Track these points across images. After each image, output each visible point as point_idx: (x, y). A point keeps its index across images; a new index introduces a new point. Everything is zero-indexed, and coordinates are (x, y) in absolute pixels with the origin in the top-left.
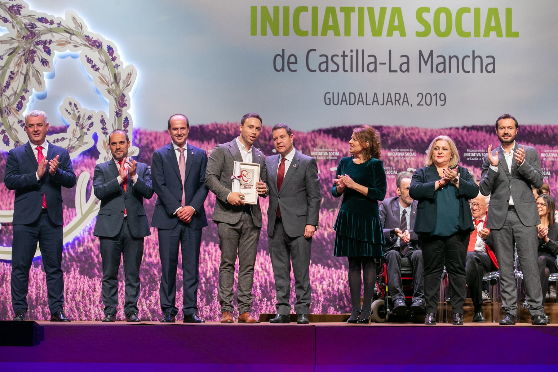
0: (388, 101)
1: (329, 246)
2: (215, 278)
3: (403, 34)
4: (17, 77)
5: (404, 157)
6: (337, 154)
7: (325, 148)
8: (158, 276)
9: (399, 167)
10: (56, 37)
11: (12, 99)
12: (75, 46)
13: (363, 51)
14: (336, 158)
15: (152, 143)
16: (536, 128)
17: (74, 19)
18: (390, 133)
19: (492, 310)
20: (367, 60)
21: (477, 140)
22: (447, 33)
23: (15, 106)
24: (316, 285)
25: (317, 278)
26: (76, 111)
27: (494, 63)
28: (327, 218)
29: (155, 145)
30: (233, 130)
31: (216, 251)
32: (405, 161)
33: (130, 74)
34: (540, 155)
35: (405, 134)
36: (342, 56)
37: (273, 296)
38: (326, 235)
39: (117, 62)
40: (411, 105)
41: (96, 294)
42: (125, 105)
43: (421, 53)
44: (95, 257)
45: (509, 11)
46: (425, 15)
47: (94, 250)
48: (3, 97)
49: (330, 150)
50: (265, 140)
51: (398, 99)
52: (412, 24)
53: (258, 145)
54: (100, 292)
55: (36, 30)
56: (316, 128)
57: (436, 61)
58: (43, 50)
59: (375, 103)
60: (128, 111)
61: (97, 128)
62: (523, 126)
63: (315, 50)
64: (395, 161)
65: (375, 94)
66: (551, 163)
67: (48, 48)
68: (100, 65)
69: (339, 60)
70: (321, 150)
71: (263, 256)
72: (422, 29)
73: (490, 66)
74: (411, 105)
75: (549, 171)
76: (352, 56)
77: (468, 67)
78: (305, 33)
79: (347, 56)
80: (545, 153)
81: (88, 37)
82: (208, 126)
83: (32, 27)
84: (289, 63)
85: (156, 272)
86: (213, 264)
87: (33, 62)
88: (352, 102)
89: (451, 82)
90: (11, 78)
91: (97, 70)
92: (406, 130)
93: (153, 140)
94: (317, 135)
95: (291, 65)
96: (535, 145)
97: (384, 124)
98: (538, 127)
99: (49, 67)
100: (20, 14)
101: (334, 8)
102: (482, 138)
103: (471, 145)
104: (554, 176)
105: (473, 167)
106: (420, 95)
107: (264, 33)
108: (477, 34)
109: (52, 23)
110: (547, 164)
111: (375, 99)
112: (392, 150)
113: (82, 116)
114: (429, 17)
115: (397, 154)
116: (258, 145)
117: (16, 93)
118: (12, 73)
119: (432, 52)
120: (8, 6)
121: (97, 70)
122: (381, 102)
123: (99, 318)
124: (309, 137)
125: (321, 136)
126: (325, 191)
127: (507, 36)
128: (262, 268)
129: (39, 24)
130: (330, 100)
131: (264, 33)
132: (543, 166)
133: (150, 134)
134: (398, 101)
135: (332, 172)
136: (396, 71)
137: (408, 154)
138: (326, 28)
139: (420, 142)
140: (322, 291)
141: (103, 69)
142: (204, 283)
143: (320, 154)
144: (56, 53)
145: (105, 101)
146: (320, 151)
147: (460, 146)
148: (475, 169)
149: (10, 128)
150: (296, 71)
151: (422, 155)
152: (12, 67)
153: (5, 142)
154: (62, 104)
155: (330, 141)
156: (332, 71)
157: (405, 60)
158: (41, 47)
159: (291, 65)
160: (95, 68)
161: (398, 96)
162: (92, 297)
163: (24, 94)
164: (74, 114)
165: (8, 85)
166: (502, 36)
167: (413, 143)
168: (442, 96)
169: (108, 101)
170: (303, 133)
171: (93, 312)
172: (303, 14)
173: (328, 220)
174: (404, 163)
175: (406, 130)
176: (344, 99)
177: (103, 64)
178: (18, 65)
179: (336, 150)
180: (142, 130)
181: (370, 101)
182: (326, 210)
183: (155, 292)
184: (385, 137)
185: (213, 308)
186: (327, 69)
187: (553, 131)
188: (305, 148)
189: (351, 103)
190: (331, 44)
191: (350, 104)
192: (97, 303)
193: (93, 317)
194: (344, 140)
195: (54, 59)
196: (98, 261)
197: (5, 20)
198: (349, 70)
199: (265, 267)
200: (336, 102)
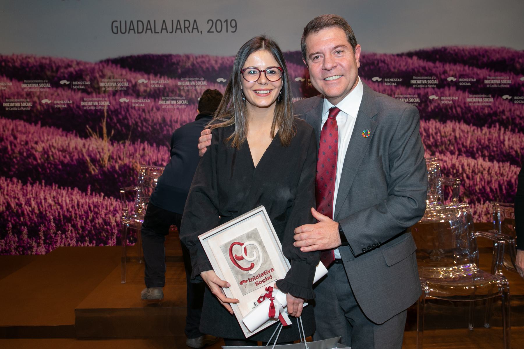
1: (121, 178)
2: (8, 213)
5: (195, 86)
6: (126, 84)
7: (113, 78)
9: (190, 96)
14: (126, 89)
18: (180, 61)
24: (109, 217)
25: (110, 211)
28: (118, 150)
30: (19, 62)
31: (8, 185)
32: (196, 90)
35: (195, 62)
37: (67, 229)
38: (117, 168)
40: (201, 32)
49: (120, 80)
50: (52, 71)
56: (104, 57)
64: (186, 91)
65: (164, 21)
70: (109, 80)
71: (55, 189)
74: (201, 32)
86: (5, 199)
88: (140, 31)
92: (197, 58)
94: (105, 66)
97: (174, 52)
106: (210, 22)
111: (164, 27)
112: (182, 79)
115: (187, 83)
122: (170, 30)
124: (97, 67)
125: (109, 67)
126: (114, 123)
128: (54, 201)
134: (187, 28)
135: (122, 103)
137: (198, 83)
139: (211, 70)
140: (115, 224)
143: (109, 84)
146: (108, 82)
151: (213, 84)
155: (118, 71)
161: (187, 23)
173: (119, 152)
174: (195, 92)
175: (197, 58)
176: (132, 28)
179: (125, 80)
181: (158, 29)
182: (116, 142)
184: (174, 66)
185: (8, 241)
189: (140, 31)
191: (138, 33)
199: (58, 200)
200: (123, 31)
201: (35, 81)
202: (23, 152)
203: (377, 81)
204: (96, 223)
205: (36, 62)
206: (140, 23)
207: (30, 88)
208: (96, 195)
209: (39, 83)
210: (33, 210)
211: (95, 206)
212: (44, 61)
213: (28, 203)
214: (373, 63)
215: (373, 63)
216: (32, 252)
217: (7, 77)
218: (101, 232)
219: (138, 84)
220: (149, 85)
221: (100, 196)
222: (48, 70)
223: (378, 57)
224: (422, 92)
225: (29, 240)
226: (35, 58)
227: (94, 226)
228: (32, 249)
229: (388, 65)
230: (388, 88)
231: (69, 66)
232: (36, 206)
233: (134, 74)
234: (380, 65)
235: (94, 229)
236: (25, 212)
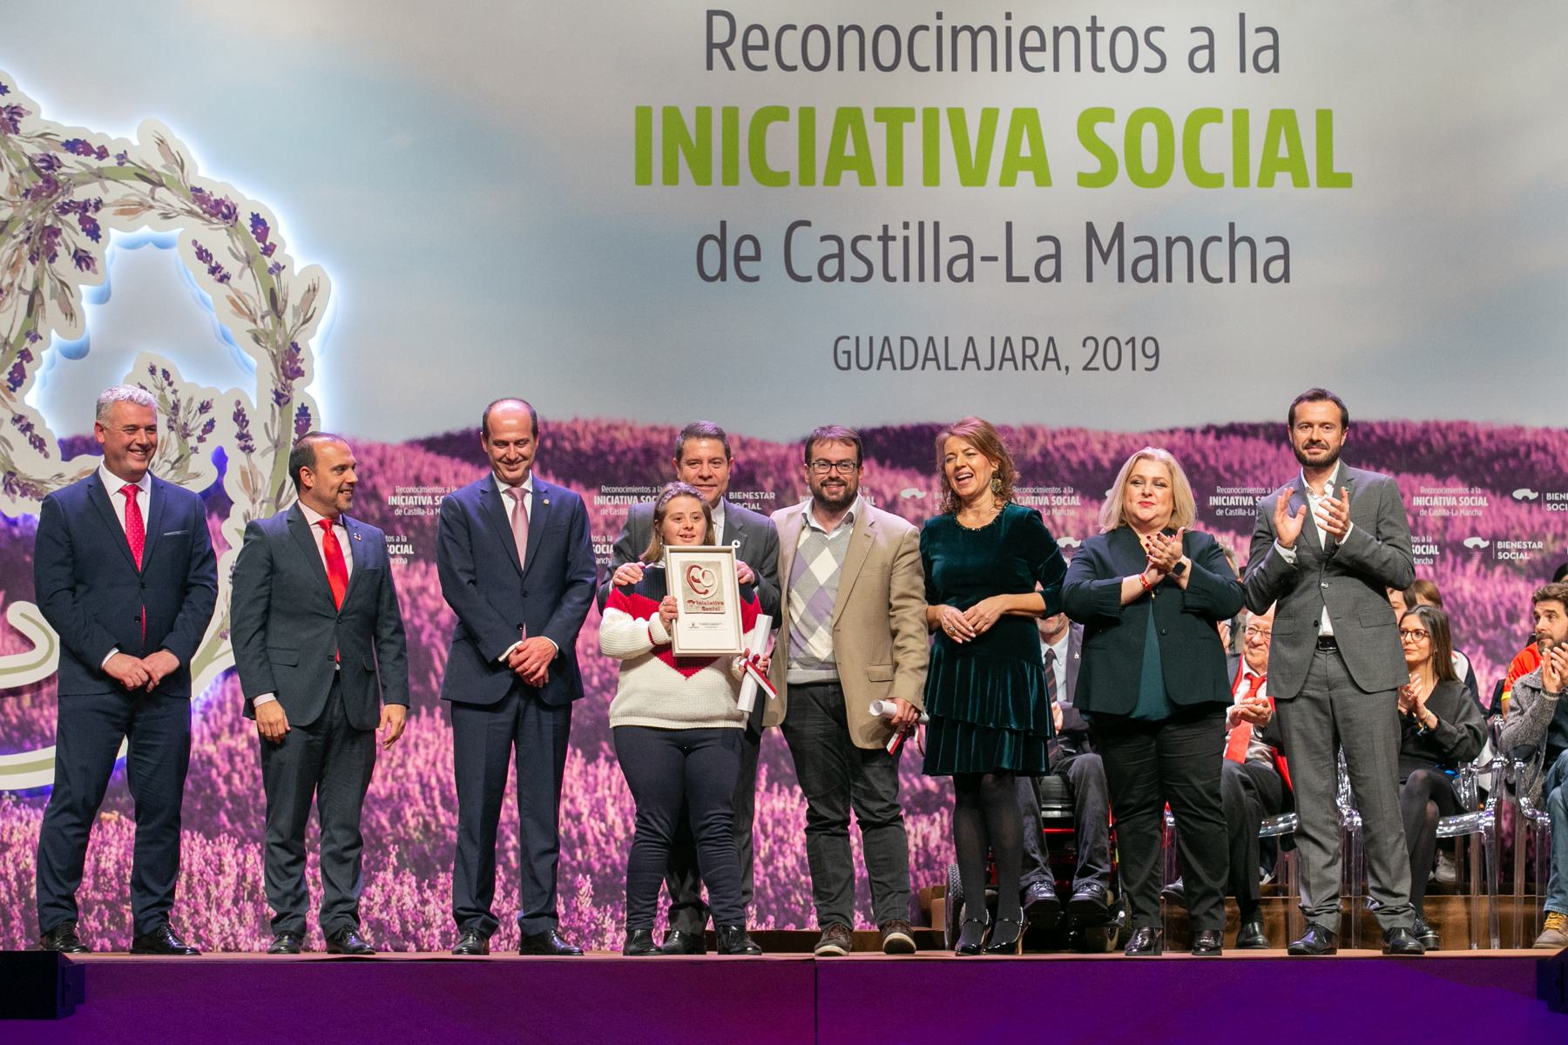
0: (1003, 359)
3: (1043, 179)
5: (1049, 507)
8: (389, 830)
10: (114, 192)
12: (166, 216)
13: (936, 225)
15: (371, 473)
16: (1400, 430)
19: (1286, 915)
20: (949, 250)
21: (1242, 463)
22: (1161, 177)
26: (168, 390)
27: (1286, 257)
29: (380, 480)
30: (589, 438)
33: (313, 290)
34: (1411, 501)
35: (1050, 447)
36: (880, 238)
41: (224, 881)
42: (299, 373)
43: (1091, 230)
44: (220, 781)
45: (1324, 119)
46: (1101, 130)
47: (219, 762)
51: (1033, 354)
52: (1066, 154)
53: (658, 480)
54: (234, 875)
55: (60, 175)
57: (1133, 250)
58: (79, 228)
59: (971, 365)
60: (307, 390)
61: (224, 433)
62: (1365, 424)
63: (808, 224)
65: (971, 339)
66: (1440, 524)
67: (93, 221)
68: (231, 266)
69: (872, 250)
72: (1093, 165)
75: (1434, 543)
76: (906, 239)
77: (1218, 266)
78: (782, 179)
79: (894, 239)
80: (1425, 495)
81: (200, 190)
83: (50, 167)
84: (738, 259)
85: (385, 822)
87: (52, 260)
88: (908, 362)
91: (224, 278)
92: (1054, 436)
93: (376, 466)
95: (744, 265)
96: (1397, 473)
98: (1404, 427)
99: (95, 272)
100: (17, 131)
101: (858, 111)
102: (1258, 457)
103: (1228, 476)
104: (1449, 556)
105: (1232, 533)
106: (1091, 343)
107: (671, 178)
108: (1241, 179)
109: (102, 154)
110: (1430, 526)
111: (971, 355)
113: (183, 404)
114: (1112, 134)
116: (658, 480)
119: (1120, 226)
121: (224, 278)
122: (985, 361)
123: (232, 946)
127: (1321, 184)
129: (67, 158)
130: (849, 357)
131: (671, 178)
132: (1420, 531)
133: (368, 451)
134: (1031, 357)
136: (1026, 279)
137: (1059, 501)
138: (838, 163)
139: (1090, 466)
141: (240, 277)
142: (514, 848)
144: (115, 235)
147: (1196, 477)
148: (1239, 540)
150: (756, 279)
151: (1095, 502)
156: (854, 279)
157: (1049, 248)
158: (73, 218)
159: (744, 265)
160: (218, 276)
161: (1030, 346)
162: (212, 888)
163: (27, 344)
166: (1307, 185)
167: (1072, 471)
168: (1150, 344)
169: (253, 361)
170: (778, 446)
171: (216, 928)
172: (774, 128)
175: (1054, 436)
176: (887, 355)
177: (241, 265)
181: (956, 360)
183: (381, 874)
186: (840, 275)
187: (1445, 437)
188: (782, 485)
190: (853, 208)
191: (903, 368)
192: (228, 904)
193: (216, 941)
194: (888, 463)
195: (108, 252)
196: (230, 792)
198: (900, 277)
200: (864, 362)
201: (629, 489)
202: (591, 675)
203: (1526, 499)
204: (777, 869)
205: (635, 439)
206: (908, 344)
207: (616, 506)
208: (780, 790)
209: (639, 495)
210: (611, 829)
211: (777, 822)
212: (655, 437)
213: (598, 811)
214: (1515, 453)
215: (1515, 453)
216: (602, 944)
217: (557, 476)
218: (787, 895)
219: (900, 500)
220: (930, 506)
221: (792, 793)
222: (666, 460)
223: (1529, 437)
225: (595, 913)
226: (631, 430)
227: (773, 876)
228: (602, 936)
229: (1554, 458)
230: (1555, 518)
232: (619, 821)
233: (889, 476)
234: (1534, 457)
235: (772, 884)
236: (590, 837)
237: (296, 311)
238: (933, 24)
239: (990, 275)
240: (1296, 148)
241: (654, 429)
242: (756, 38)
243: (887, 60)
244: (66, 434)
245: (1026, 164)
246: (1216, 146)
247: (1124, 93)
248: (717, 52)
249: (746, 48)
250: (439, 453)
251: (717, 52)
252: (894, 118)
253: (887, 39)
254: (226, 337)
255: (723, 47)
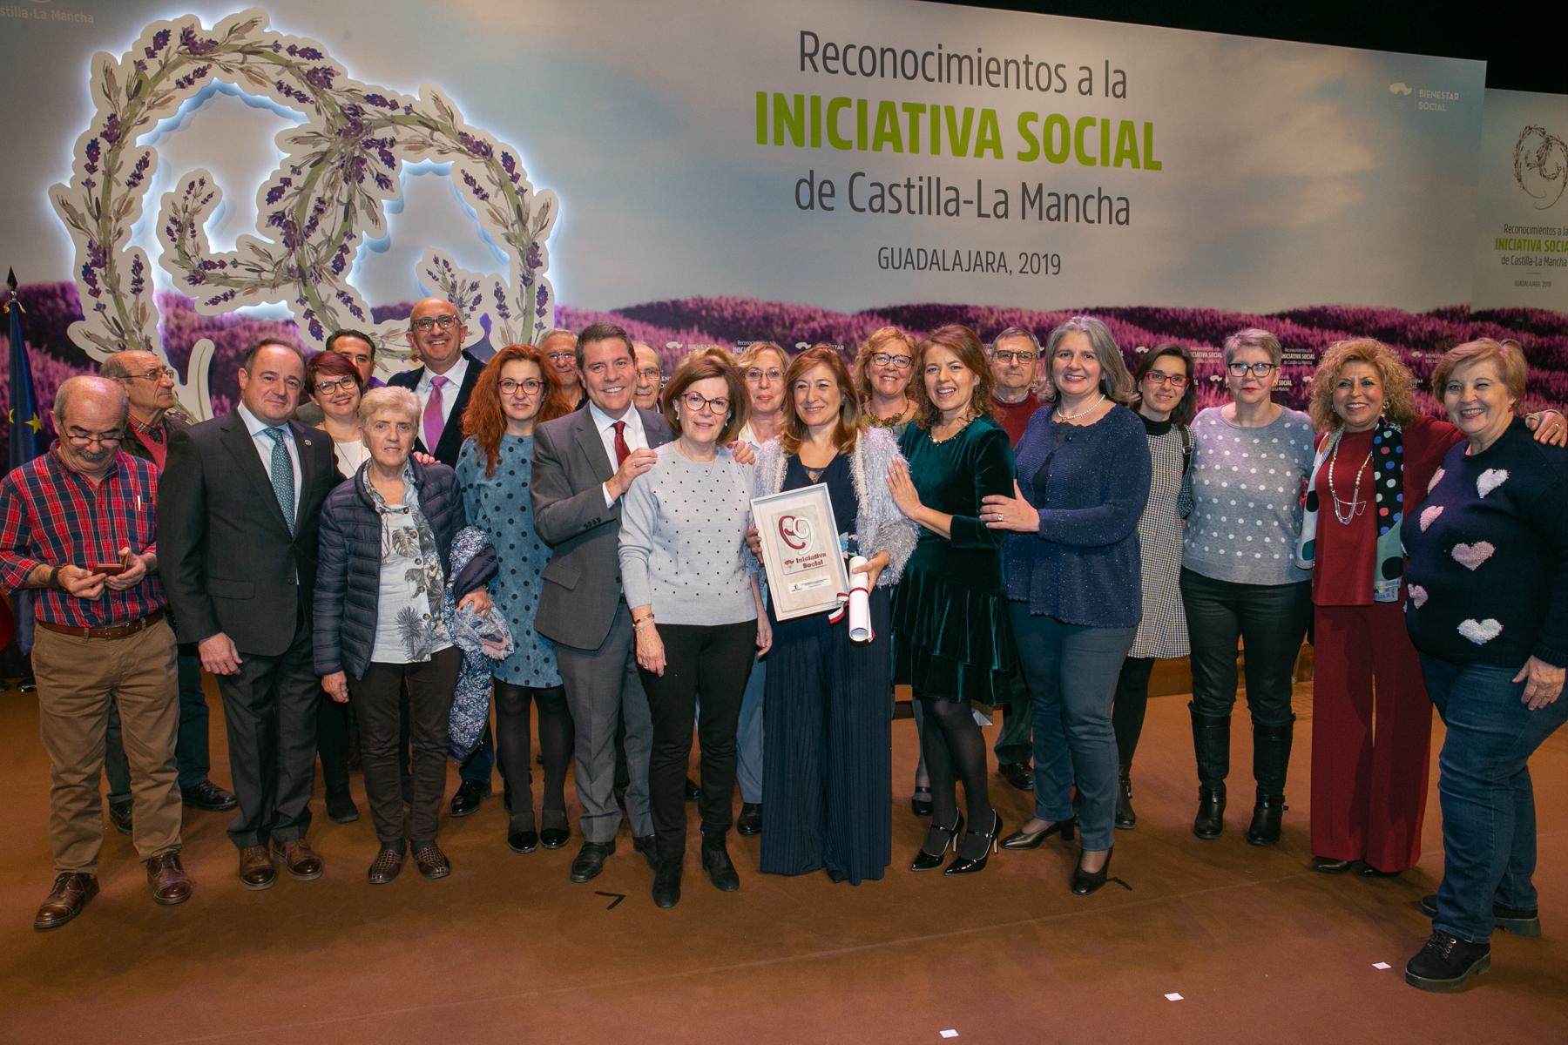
4: (330, 210)
10: (404, 133)
11: (323, 253)
12: (441, 152)
17: (437, 99)
20: (946, 195)
22: (1062, 158)
23: (330, 264)
26: (448, 275)
27: (1127, 209)
33: (546, 207)
39: (520, 183)
42: (539, 264)
45: (1148, 127)
46: (1031, 125)
48: (306, 247)
50: (784, 327)
52: (1012, 140)
55: (364, 119)
56: (867, 307)
57: (1048, 201)
61: (489, 306)
68: (489, 188)
69: (901, 193)
72: (1026, 148)
73: (1122, 216)
78: (846, 145)
82: (686, 303)
83: (356, 114)
84: (821, 195)
87: (360, 181)
88: (922, 265)
89: (1069, 236)
90: (319, 211)
91: (485, 197)
97: (971, 302)
100: (330, 87)
107: (779, 140)
108: (1105, 162)
109: (394, 106)
114: (1036, 128)
117: (330, 239)
118: (320, 200)
120: (306, 69)
121: (485, 197)
122: (966, 266)
124: (854, 322)
129: (369, 108)
130: (887, 261)
131: (779, 140)
144: (405, 164)
145: (501, 257)
149: (323, 306)
152: (319, 190)
153: (313, 334)
154: (420, 262)
157: (1001, 197)
158: (374, 151)
163: (345, 241)
164: (445, 280)
165: (314, 224)
172: (842, 111)
178: (332, 185)
180: (570, 309)
181: (949, 265)
186: (882, 208)
190: (889, 166)
197: (302, 98)
212: (771, 310)
217: (710, 334)
224: (1295, 371)
231: (811, 318)
237: (535, 223)
238: (936, 52)
239: (968, 211)
240: (1132, 145)
241: (770, 304)
242: (831, 52)
243: (910, 73)
244: (377, 304)
245: (988, 144)
246: (1092, 136)
247: (1045, 104)
248: (807, 59)
249: (825, 58)
250: (633, 319)
251: (807, 59)
252: (914, 110)
253: (909, 58)
254: (486, 239)
255: (811, 56)
